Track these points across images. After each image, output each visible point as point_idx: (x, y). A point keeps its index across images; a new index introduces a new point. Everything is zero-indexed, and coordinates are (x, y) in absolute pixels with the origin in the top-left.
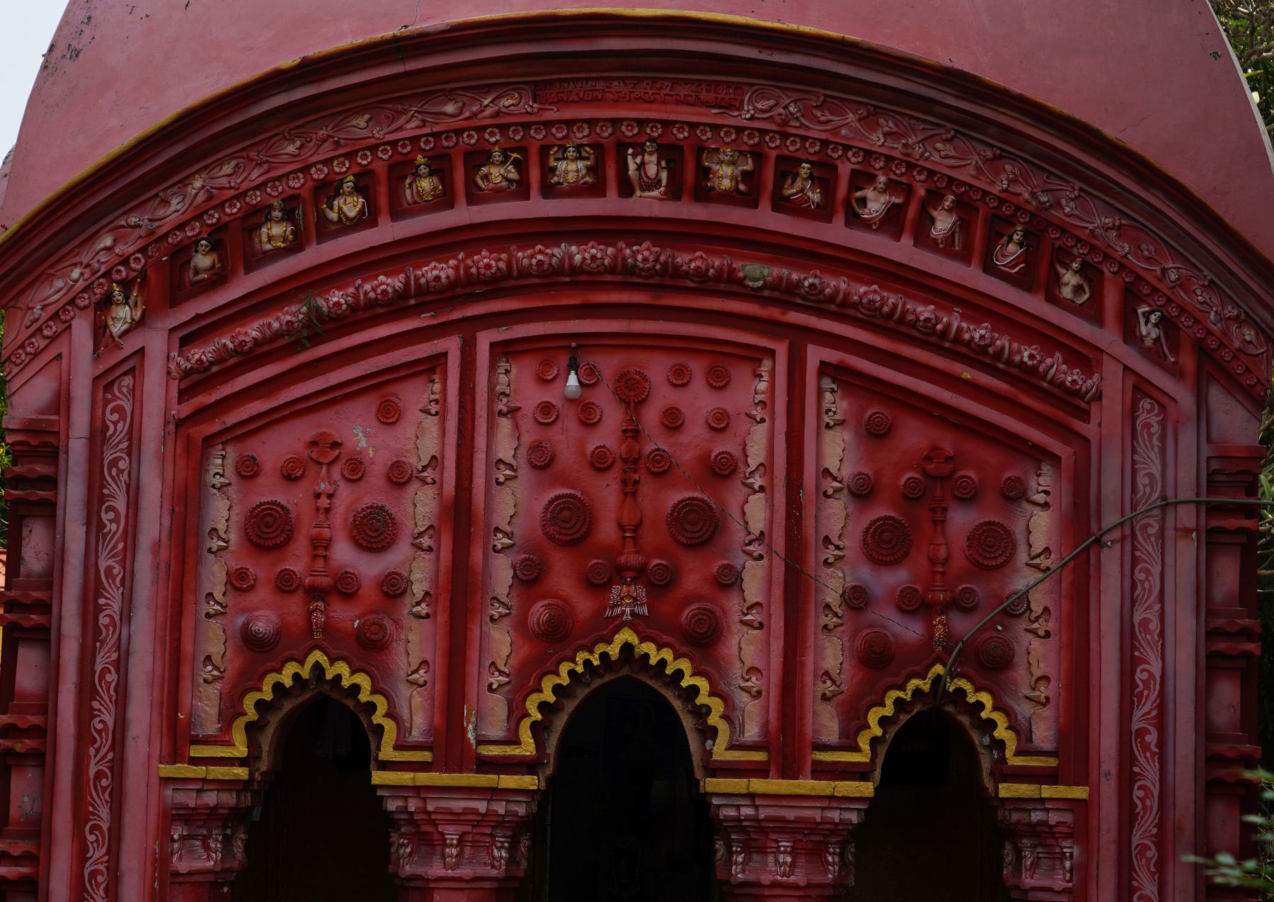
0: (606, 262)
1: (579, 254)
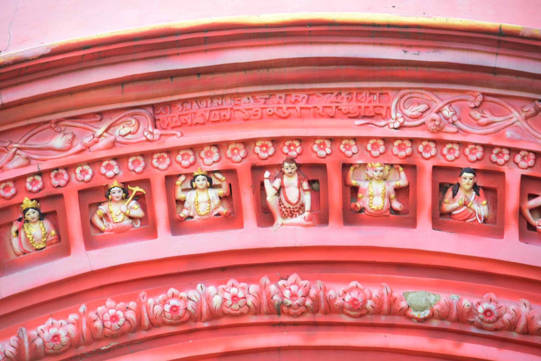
0: (250, 301)
1: (217, 294)
